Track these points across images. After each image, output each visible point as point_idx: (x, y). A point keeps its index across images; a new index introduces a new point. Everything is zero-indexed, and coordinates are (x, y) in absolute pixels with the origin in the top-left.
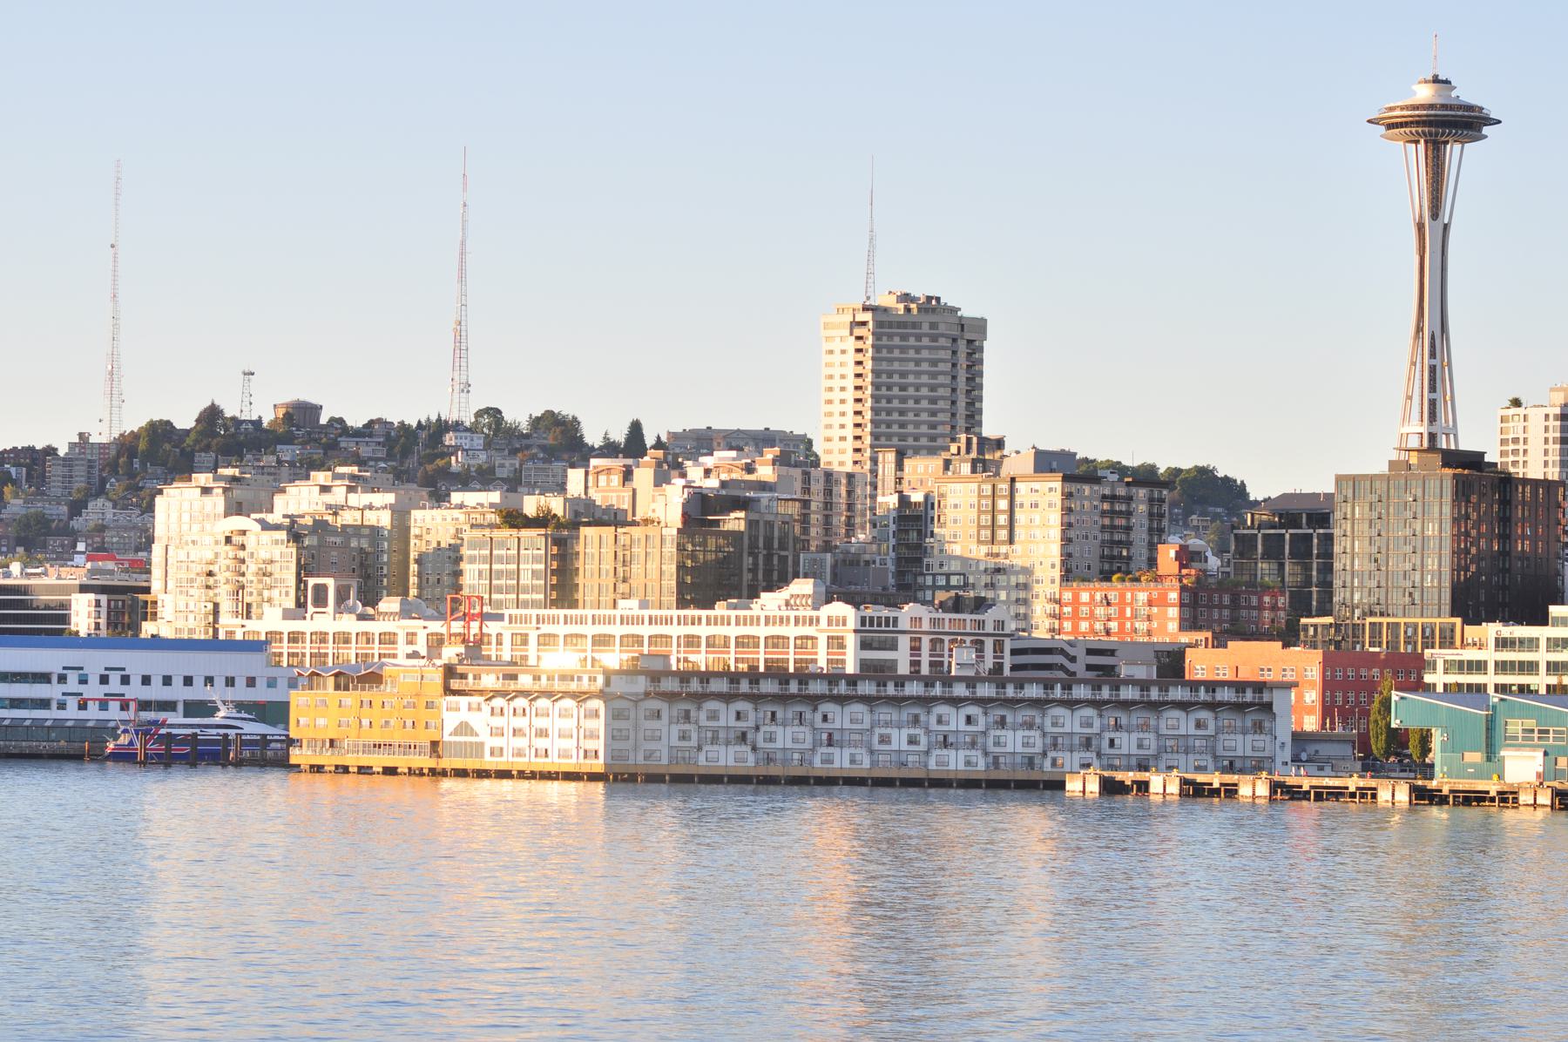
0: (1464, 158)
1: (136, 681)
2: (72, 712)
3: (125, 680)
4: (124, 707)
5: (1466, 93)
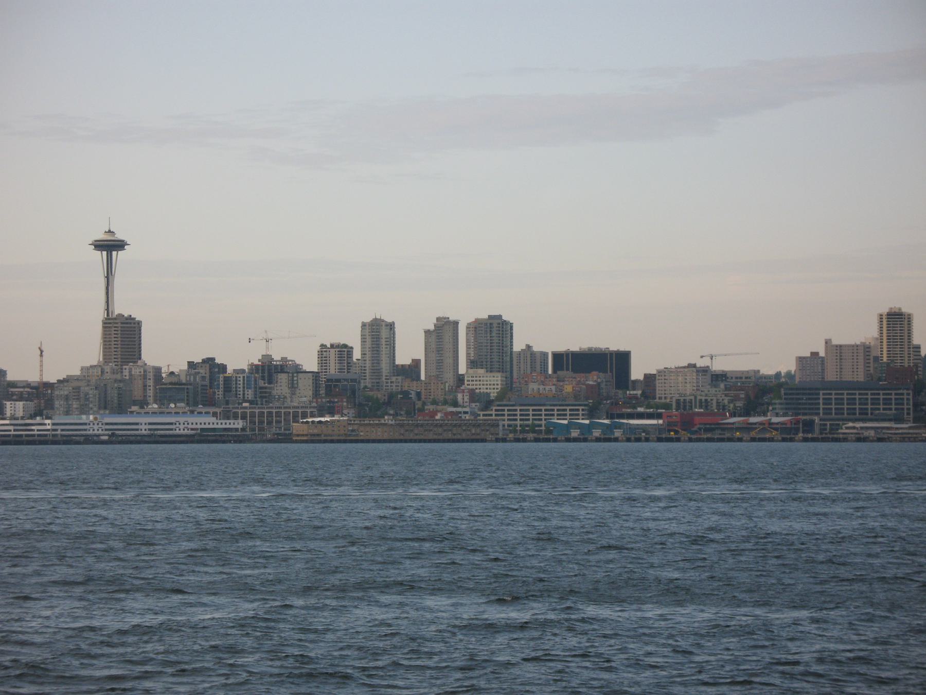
0: (120, 257)
1: (190, 424)
2: (178, 431)
3: (188, 424)
4: (188, 430)
5: (119, 236)
